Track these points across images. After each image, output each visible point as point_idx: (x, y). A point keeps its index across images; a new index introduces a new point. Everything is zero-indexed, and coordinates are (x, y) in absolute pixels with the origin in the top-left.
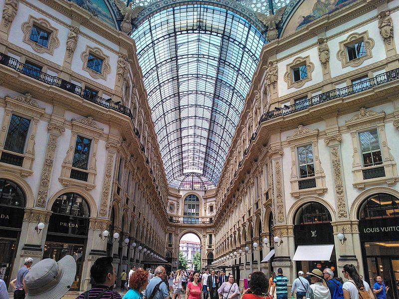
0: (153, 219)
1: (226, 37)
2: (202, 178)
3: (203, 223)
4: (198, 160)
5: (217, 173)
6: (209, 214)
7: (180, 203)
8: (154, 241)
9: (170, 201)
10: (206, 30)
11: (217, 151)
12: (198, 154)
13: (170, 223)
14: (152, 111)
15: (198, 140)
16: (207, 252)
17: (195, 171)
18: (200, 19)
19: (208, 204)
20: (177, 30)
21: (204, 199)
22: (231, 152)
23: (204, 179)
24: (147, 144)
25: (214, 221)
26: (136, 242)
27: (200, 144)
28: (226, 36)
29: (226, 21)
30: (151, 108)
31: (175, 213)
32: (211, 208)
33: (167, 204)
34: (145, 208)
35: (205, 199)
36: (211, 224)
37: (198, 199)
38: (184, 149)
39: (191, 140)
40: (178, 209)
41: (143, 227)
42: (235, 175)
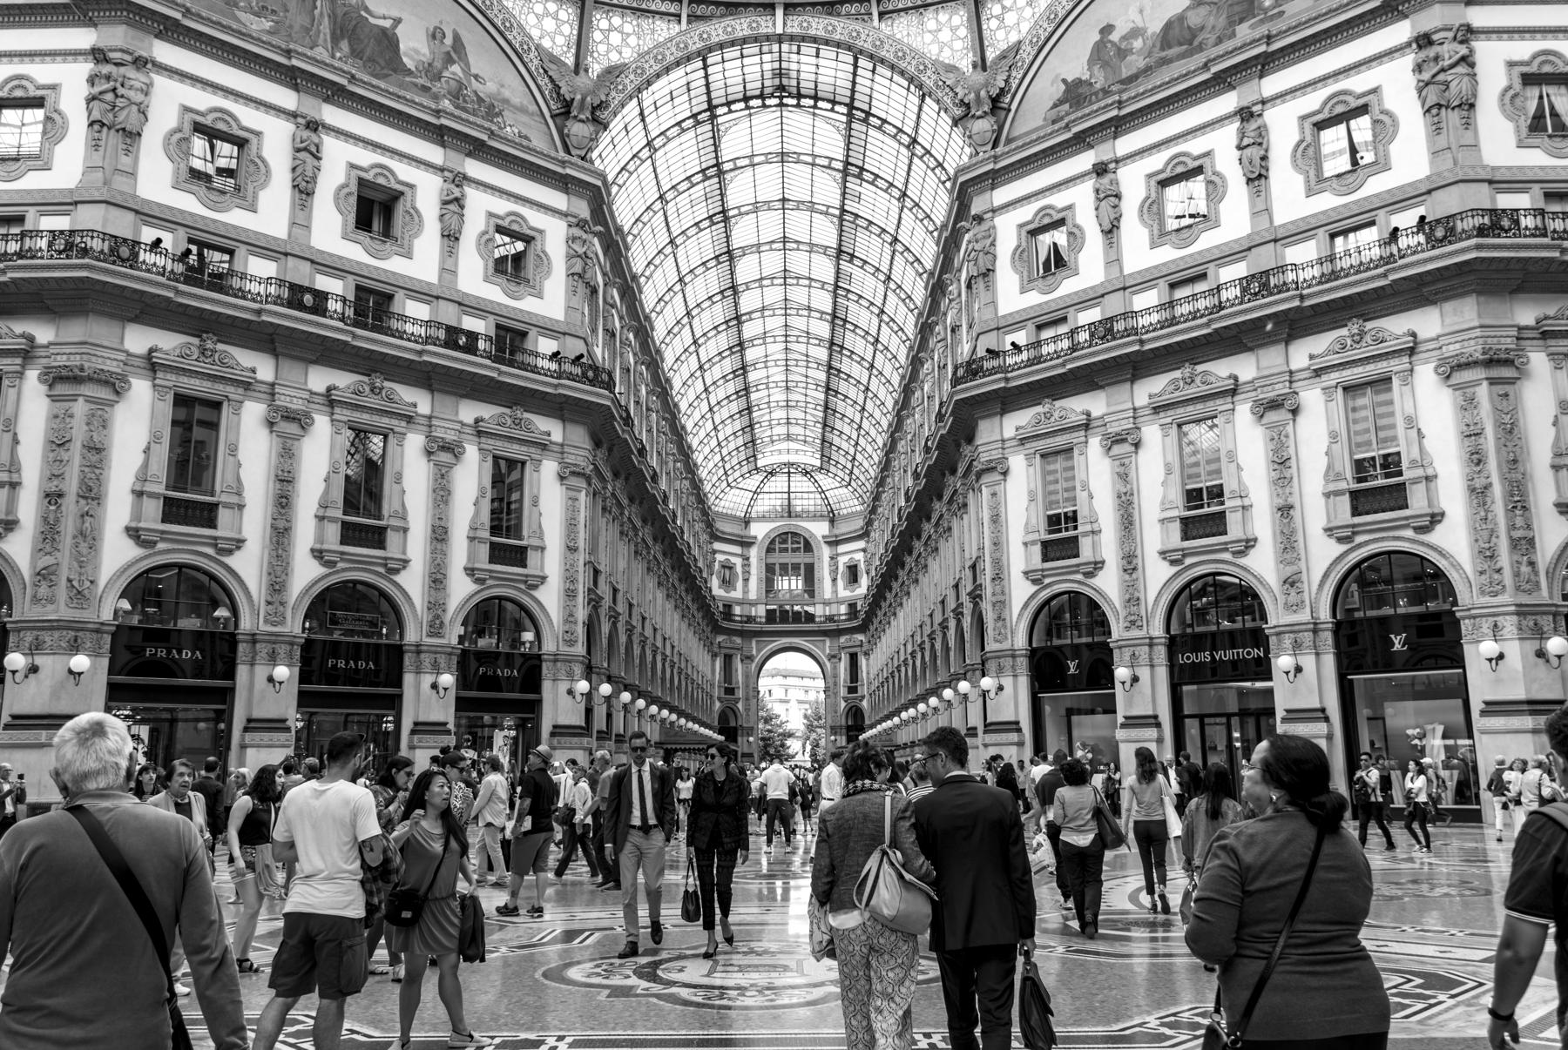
0: (676, 624)
1: (856, 113)
2: (819, 477)
3: (830, 619)
4: (803, 371)
5: (877, 414)
6: (844, 593)
7: (754, 561)
8: (683, 683)
9: (720, 557)
10: (799, 96)
11: (874, 332)
12: (802, 348)
13: (725, 624)
14: (630, 238)
15: (798, 295)
16: (843, 704)
17: (793, 458)
18: (780, 69)
19: (843, 560)
20: (715, 102)
21: (829, 543)
22: (925, 330)
23: (826, 481)
24: (647, 417)
25: (862, 616)
26: (609, 680)
27: (809, 308)
28: (858, 109)
29: (855, 74)
30: (626, 229)
31: (737, 594)
32: (853, 573)
33: (710, 566)
34: (655, 599)
35: (834, 542)
36: (855, 623)
37: (808, 547)
38: (750, 330)
39: (774, 295)
40: (746, 580)
41: (643, 642)
42: (940, 417)
